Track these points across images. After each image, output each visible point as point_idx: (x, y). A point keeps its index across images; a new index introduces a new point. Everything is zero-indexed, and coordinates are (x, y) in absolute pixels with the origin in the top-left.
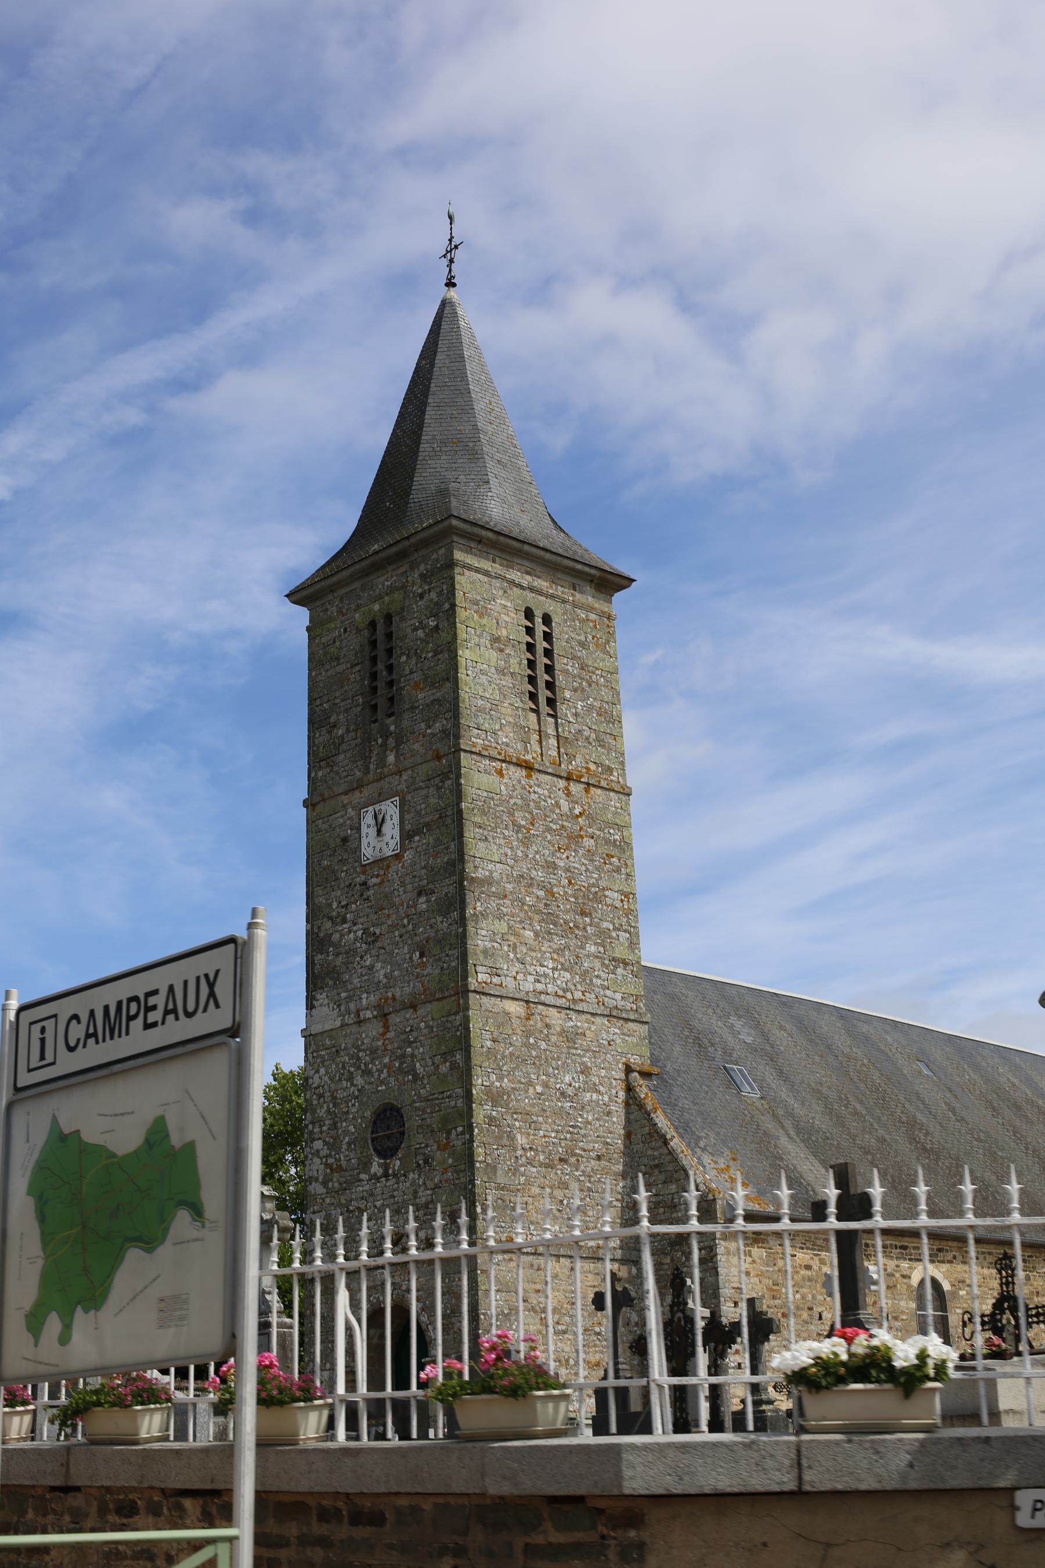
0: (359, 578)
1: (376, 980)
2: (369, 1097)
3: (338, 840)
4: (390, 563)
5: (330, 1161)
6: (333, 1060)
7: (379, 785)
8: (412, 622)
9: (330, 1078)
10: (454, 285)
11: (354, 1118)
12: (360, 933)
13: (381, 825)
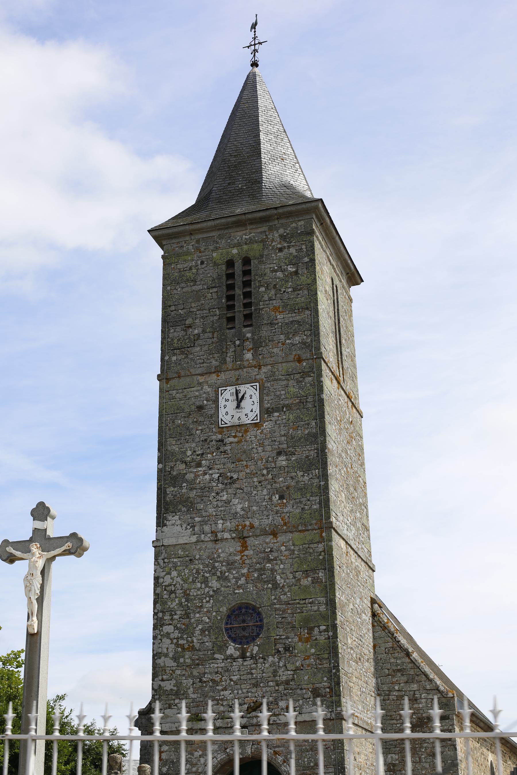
0: (219, 229)
1: (233, 511)
2: (225, 597)
3: (193, 407)
4: (251, 224)
5: (181, 642)
6: (187, 566)
7: (237, 373)
8: (272, 266)
9: (183, 580)
10: (257, 65)
11: (208, 611)
12: (216, 476)
13: (241, 401)
